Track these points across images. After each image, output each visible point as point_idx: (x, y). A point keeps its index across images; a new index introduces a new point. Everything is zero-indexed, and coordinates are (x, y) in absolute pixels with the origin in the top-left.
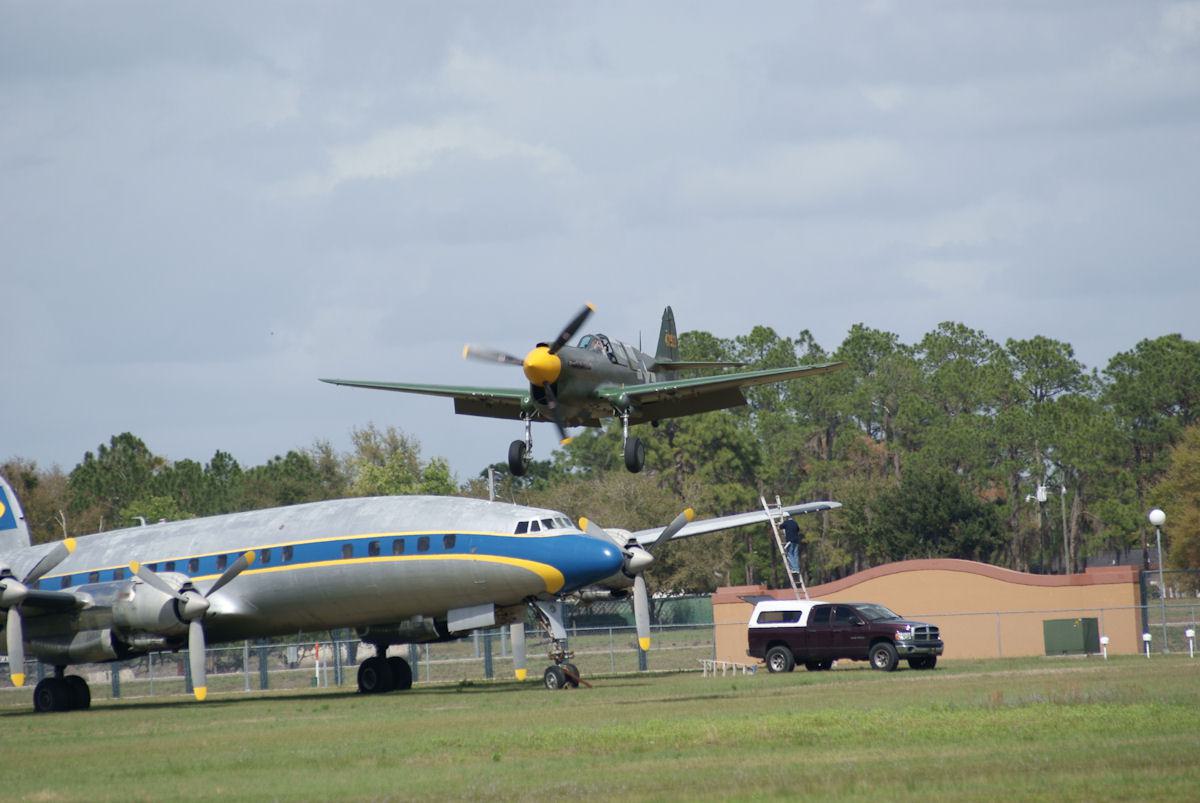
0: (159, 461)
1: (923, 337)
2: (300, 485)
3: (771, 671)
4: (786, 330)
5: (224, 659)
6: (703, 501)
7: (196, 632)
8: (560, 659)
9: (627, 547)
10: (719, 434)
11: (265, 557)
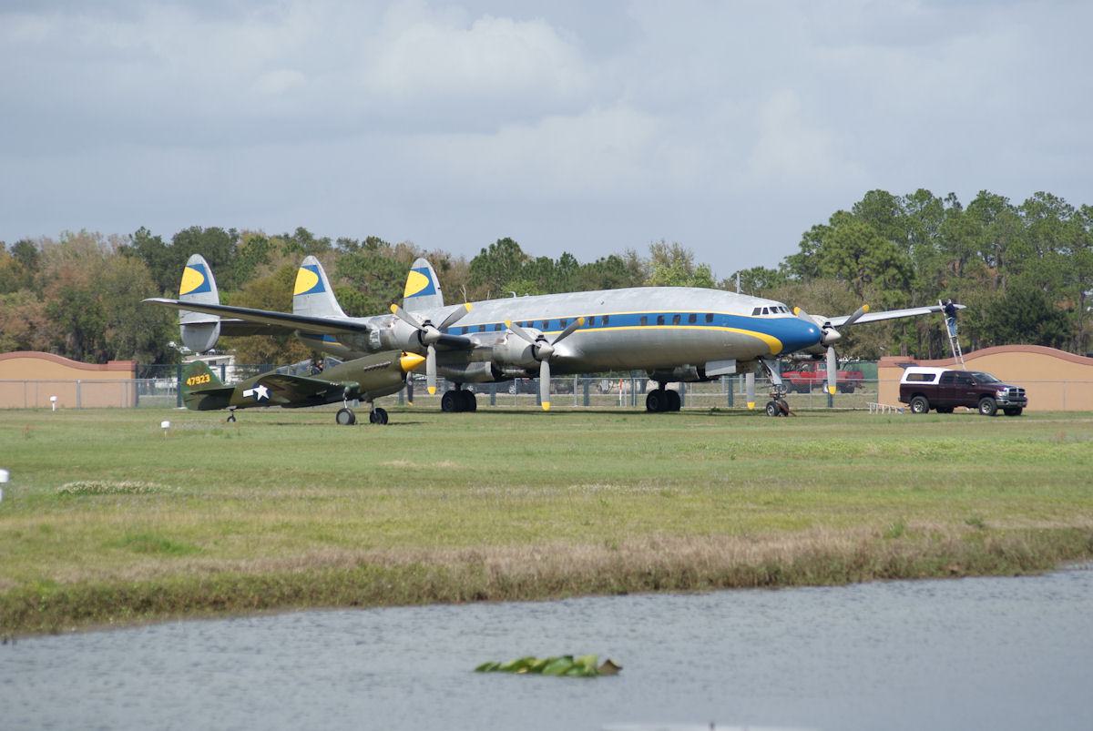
0: (525, 257)
1: (1024, 201)
2: (616, 278)
3: (914, 412)
4: (939, 192)
5: (562, 386)
6: (875, 301)
7: (545, 368)
8: (777, 397)
9: (824, 327)
10: (889, 257)
11: (591, 322)
